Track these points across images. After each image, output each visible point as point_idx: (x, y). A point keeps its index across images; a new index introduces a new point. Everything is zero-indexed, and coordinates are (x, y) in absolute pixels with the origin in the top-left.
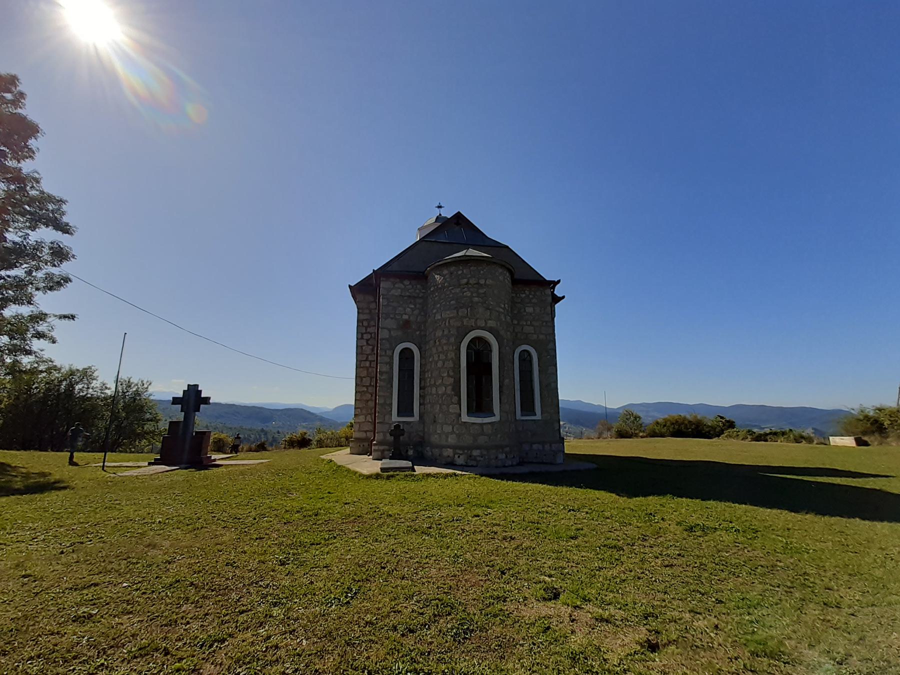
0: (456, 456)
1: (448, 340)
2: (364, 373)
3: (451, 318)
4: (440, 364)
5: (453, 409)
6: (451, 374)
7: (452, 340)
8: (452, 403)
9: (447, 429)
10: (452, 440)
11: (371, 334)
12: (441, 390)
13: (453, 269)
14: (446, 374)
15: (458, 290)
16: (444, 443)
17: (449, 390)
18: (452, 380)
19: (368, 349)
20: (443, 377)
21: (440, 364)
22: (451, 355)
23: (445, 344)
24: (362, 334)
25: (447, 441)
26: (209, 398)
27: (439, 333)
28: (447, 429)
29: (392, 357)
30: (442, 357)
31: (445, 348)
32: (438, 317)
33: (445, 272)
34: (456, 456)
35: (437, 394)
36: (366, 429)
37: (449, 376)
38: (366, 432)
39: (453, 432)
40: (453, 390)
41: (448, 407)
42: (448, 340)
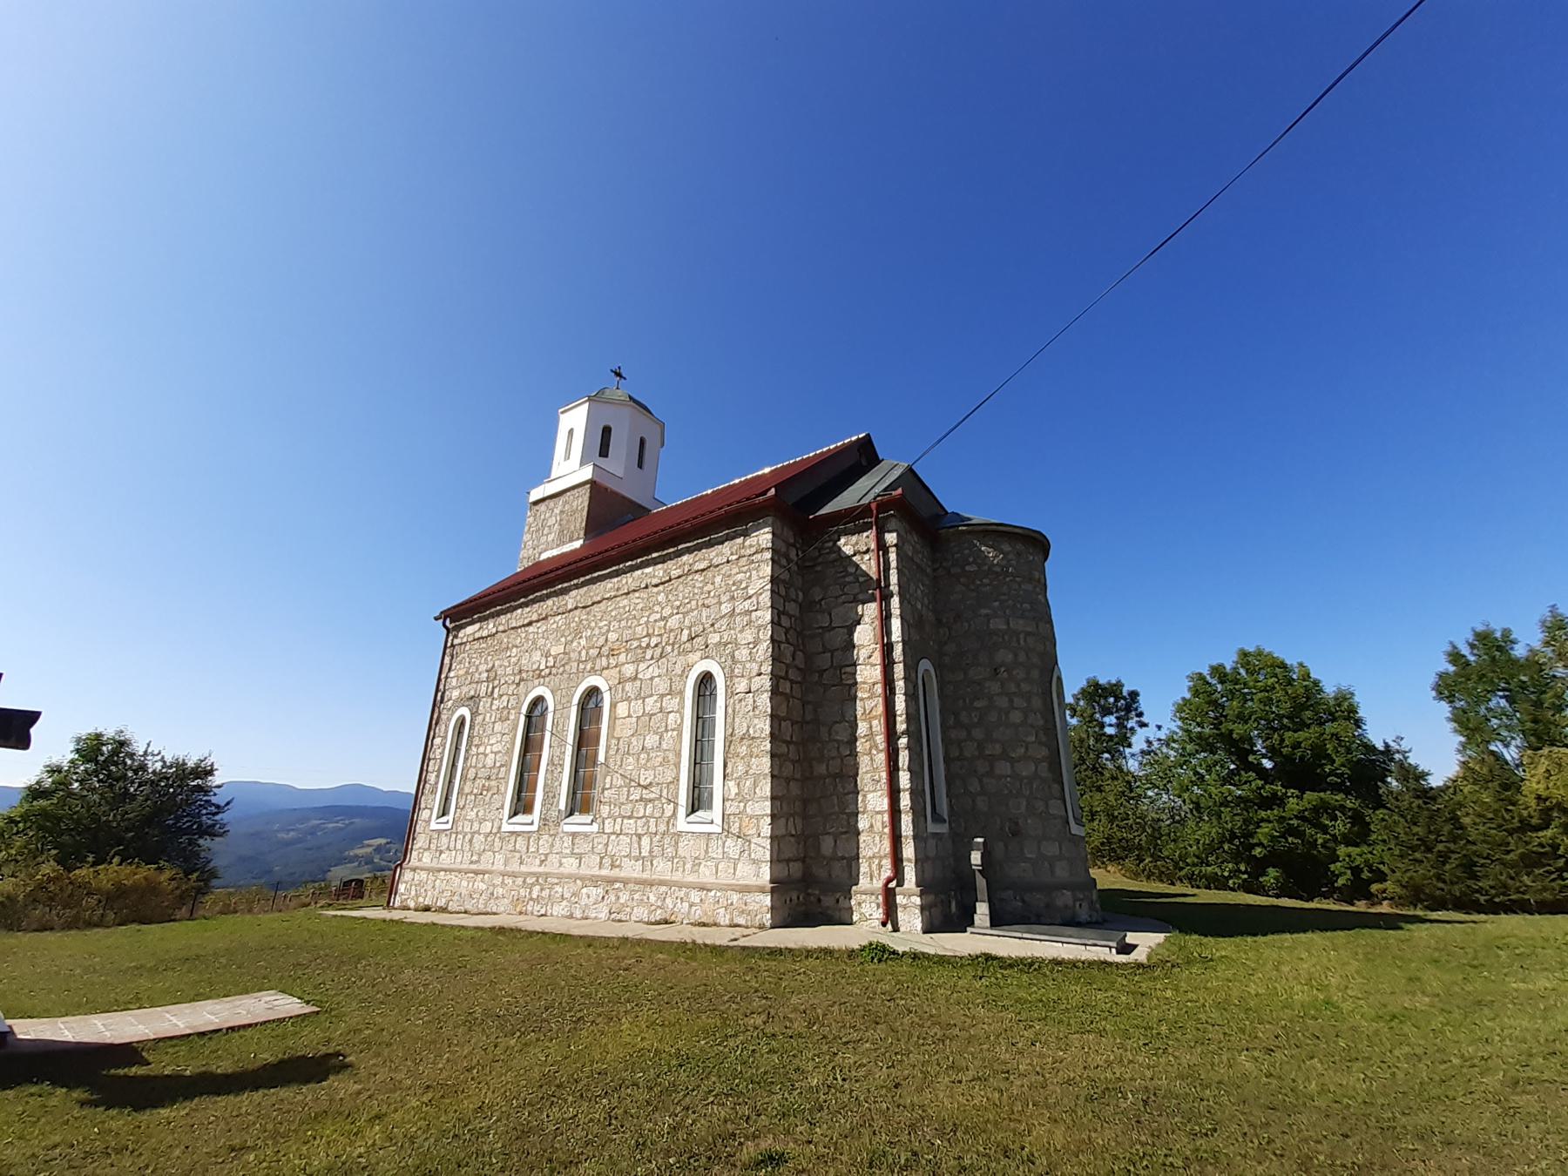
2: (783, 713)
3: (1028, 634)
4: (1016, 717)
5: (1055, 808)
7: (1035, 674)
9: (1051, 849)
10: (1062, 872)
11: (790, 617)
12: (1026, 770)
13: (1019, 546)
15: (1029, 587)
18: (1044, 752)
19: (787, 650)
21: (1016, 717)
22: (1037, 703)
25: (1053, 872)
27: (1004, 656)
28: (1051, 849)
29: (916, 686)
30: (1018, 702)
31: (1025, 687)
32: (998, 624)
33: (1006, 547)
36: (788, 855)
37: (1040, 743)
38: (788, 861)
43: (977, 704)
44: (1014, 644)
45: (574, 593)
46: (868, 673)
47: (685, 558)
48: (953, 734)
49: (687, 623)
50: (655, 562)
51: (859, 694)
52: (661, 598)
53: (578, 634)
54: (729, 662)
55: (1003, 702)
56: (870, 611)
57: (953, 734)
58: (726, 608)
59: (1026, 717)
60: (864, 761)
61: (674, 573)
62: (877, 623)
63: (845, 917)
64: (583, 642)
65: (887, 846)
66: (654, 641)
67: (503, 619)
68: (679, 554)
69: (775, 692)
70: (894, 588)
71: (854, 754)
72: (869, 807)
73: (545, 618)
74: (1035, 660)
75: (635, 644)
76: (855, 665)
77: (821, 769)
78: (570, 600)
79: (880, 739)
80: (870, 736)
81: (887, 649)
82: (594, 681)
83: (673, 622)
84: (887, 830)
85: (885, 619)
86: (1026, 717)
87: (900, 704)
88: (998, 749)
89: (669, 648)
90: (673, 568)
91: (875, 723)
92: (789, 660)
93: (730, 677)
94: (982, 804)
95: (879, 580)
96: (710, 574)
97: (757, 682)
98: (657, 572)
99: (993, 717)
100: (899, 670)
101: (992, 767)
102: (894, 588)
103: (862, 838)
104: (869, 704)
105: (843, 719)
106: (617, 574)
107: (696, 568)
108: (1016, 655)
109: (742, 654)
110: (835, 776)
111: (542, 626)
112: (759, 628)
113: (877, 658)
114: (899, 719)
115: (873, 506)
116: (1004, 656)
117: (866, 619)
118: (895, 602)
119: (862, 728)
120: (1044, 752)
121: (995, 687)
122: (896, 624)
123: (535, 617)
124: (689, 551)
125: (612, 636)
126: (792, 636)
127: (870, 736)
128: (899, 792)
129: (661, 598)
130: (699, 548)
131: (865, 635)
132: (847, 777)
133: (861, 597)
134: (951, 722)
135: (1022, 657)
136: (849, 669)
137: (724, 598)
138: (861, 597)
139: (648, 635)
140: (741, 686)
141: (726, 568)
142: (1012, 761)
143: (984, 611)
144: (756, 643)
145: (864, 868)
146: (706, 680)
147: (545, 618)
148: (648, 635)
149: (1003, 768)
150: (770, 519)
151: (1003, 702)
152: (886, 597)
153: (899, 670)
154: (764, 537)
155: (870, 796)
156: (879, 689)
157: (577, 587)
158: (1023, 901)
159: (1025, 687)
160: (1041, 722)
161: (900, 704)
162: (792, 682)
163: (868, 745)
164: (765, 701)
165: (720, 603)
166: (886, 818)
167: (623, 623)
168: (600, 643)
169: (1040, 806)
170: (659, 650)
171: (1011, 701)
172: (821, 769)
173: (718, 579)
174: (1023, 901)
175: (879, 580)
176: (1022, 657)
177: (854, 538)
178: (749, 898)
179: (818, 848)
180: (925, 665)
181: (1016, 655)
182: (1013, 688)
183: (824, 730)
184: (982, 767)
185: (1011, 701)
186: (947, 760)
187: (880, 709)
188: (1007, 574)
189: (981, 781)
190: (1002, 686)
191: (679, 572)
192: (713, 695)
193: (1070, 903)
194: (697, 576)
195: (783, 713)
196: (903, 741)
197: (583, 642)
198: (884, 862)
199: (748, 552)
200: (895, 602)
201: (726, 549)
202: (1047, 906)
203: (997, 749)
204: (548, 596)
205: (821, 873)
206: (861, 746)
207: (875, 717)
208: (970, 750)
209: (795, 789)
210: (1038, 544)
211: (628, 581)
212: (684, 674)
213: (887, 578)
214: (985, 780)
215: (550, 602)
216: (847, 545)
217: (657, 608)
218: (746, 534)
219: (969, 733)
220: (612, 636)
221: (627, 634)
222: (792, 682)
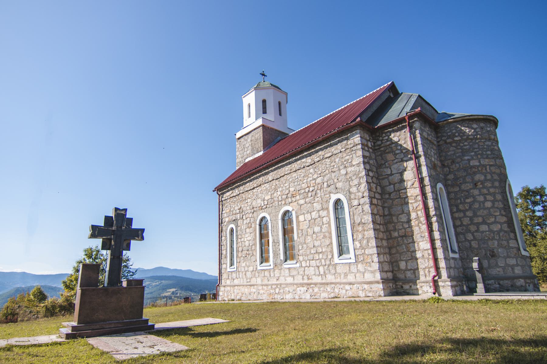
0: (527, 285)
1: (493, 183)
2: (375, 212)
3: (491, 166)
5: (512, 244)
6: (504, 213)
7: (497, 184)
8: (511, 239)
9: (512, 262)
10: (518, 271)
12: (496, 227)
14: (498, 214)
15: (490, 143)
16: (509, 273)
17: (505, 227)
18: (504, 219)
20: (495, 216)
21: (488, 204)
22: (499, 197)
23: (490, 187)
24: (368, 171)
25: (514, 272)
26: (143, 230)
27: (479, 177)
28: (512, 262)
29: (437, 195)
30: (489, 197)
31: (492, 190)
33: (475, 126)
34: (527, 285)
35: (491, 231)
36: (386, 269)
37: (502, 215)
38: (386, 272)
39: (517, 265)
40: (509, 227)
41: (508, 242)
42: (493, 183)
43: (468, 200)
44: (484, 171)
45: (271, 174)
46: (413, 192)
47: (320, 153)
48: (457, 215)
49: (325, 179)
50: (306, 156)
51: (410, 201)
52: (312, 171)
53: (276, 190)
54: (348, 194)
55: (481, 198)
56: (410, 164)
57: (457, 215)
58: (343, 172)
59: (494, 204)
60: (416, 230)
61: (316, 160)
62: (415, 169)
63: (415, 292)
64: (279, 193)
65: (431, 263)
66: (311, 189)
67: (241, 188)
68: (317, 152)
69: (371, 203)
70: (421, 153)
71: (410, 227)
72: (421, 248)
73: (260, 185)
74: (496, 177)
75: (303, 191)
76: (406, 189)
77: (396, 234)
78: (270, 177)
79: (423, 219)
80: (418, 218)
81: (421, 181)
82: (289, 208)
83: (319, 180)
84: (431, 257)
85: (418, 168)
86: (494, 204)
87: (431, 203)
88: (480, 220)
89: (318, 191)
90: (316, 158)
91: (419, 213)
92: (374, 190)
93: (349, 200)
94: (474, 244)
95: (413, 151)
96: (333, 158)
97: (362, 201)
98: (309, 160)
99: (476, 206)
100: (428, 189)
101: (478, 228)
102: (421, 153)
103: (419, 261)
104: (415, 205)
105: (403, 212)
106: (290, 163)
107: (326, 156)
108: (485, 176)
109: (354, 190)
110: (402, 237)
111: (259, 189)
112: (360, 178)
113: (417, 184)
114: (431, 210)
115: (406, 118)
116: (479, 177)
117: (409, 168)
118: (422, 160)
119: (413, 215)
120: (504, 219)
121: (476, 192)
122: (424, 169)
123: (255, 186)
124: (321, 149)
125: (292, 189)
126: (375, 180)
127: (418, 218)
128: (434, 240)
129: (312, 171)
130: (326, 148)
131: (409, 176)
132: (408, 236)
133: (405, 159)
134: (455, 210)
135: (489, 177)
136: (403, 191)
137: (341, 167)
138: (405, 159)
139: (308, 187)
140: (355, 203)
141: (340, 155)
142: (489, 224)
143: (466, 158)
144: (360, 184)
145: (421, 272)
146: (338, 202)
147: (260, 185)
148: (308, 187)
149: (484, 228)
150: (358, 131)
151: (481, 198)
152: (417, 157)
153: (428, 189)
154: (356, 139)
155: (420, 243)
156: (419, 198)
157: (272, 171)
158: (499, 284)
159: (492, 190)
160: (502, 206)
161: (431, 203)
162: (377, 199)
163: (417, 222)
164: (367, 208)
165: (339, 170)
166: (430, 252)
167: (296, 183)
168: (286, 193)
169: (505, 243)
170: (314, 193)
171: (485, 198)
172: (396, 234)
173: (337, 160)
174: (499, 284)
175: (413, 151)
176: (489, 177)
177: (398, 133)
178: (373, 286)
179: (398, 266)
180: (440, 185)
181: (485, 176)
182: (485, 191)
183: (394, 218)
184: (473, 228)
185: (485, 198)
186: (455, 227)
187: (421, 206)
188: (477, 139)
189: (473, 235)
190: (480, 191)
191: (318, 159)
192: (342, 208)
193: (524, 284)
194: (327, 160)
195: (375, 212)
196: (434, 219)
197: (279, 193)
198: (431, 270)
199: (350, 146)
200: (422, 160)
201: (339, 146)
202: (512, 286)
203: (480, 220)
204: (260, 176)
205: (401, 276)
206: (413, 223)
207: (419, 210)
208: (466, 221)
209: (385, 243)
210: (492, 122)
211: (295, 166)
212: (328, 202)
213: (417, 149)
214: (475, 234)
215: (261, 179)
216: (395, 137)
217: (310, 175)
218: (347, 139)
219: (465, 214)
220: (292, 189)
221: (298, 188)
222: (377, 199)
